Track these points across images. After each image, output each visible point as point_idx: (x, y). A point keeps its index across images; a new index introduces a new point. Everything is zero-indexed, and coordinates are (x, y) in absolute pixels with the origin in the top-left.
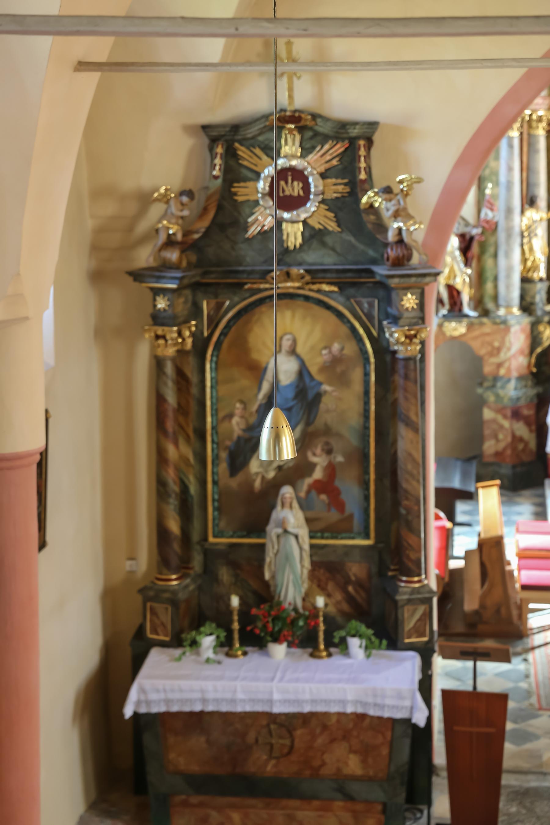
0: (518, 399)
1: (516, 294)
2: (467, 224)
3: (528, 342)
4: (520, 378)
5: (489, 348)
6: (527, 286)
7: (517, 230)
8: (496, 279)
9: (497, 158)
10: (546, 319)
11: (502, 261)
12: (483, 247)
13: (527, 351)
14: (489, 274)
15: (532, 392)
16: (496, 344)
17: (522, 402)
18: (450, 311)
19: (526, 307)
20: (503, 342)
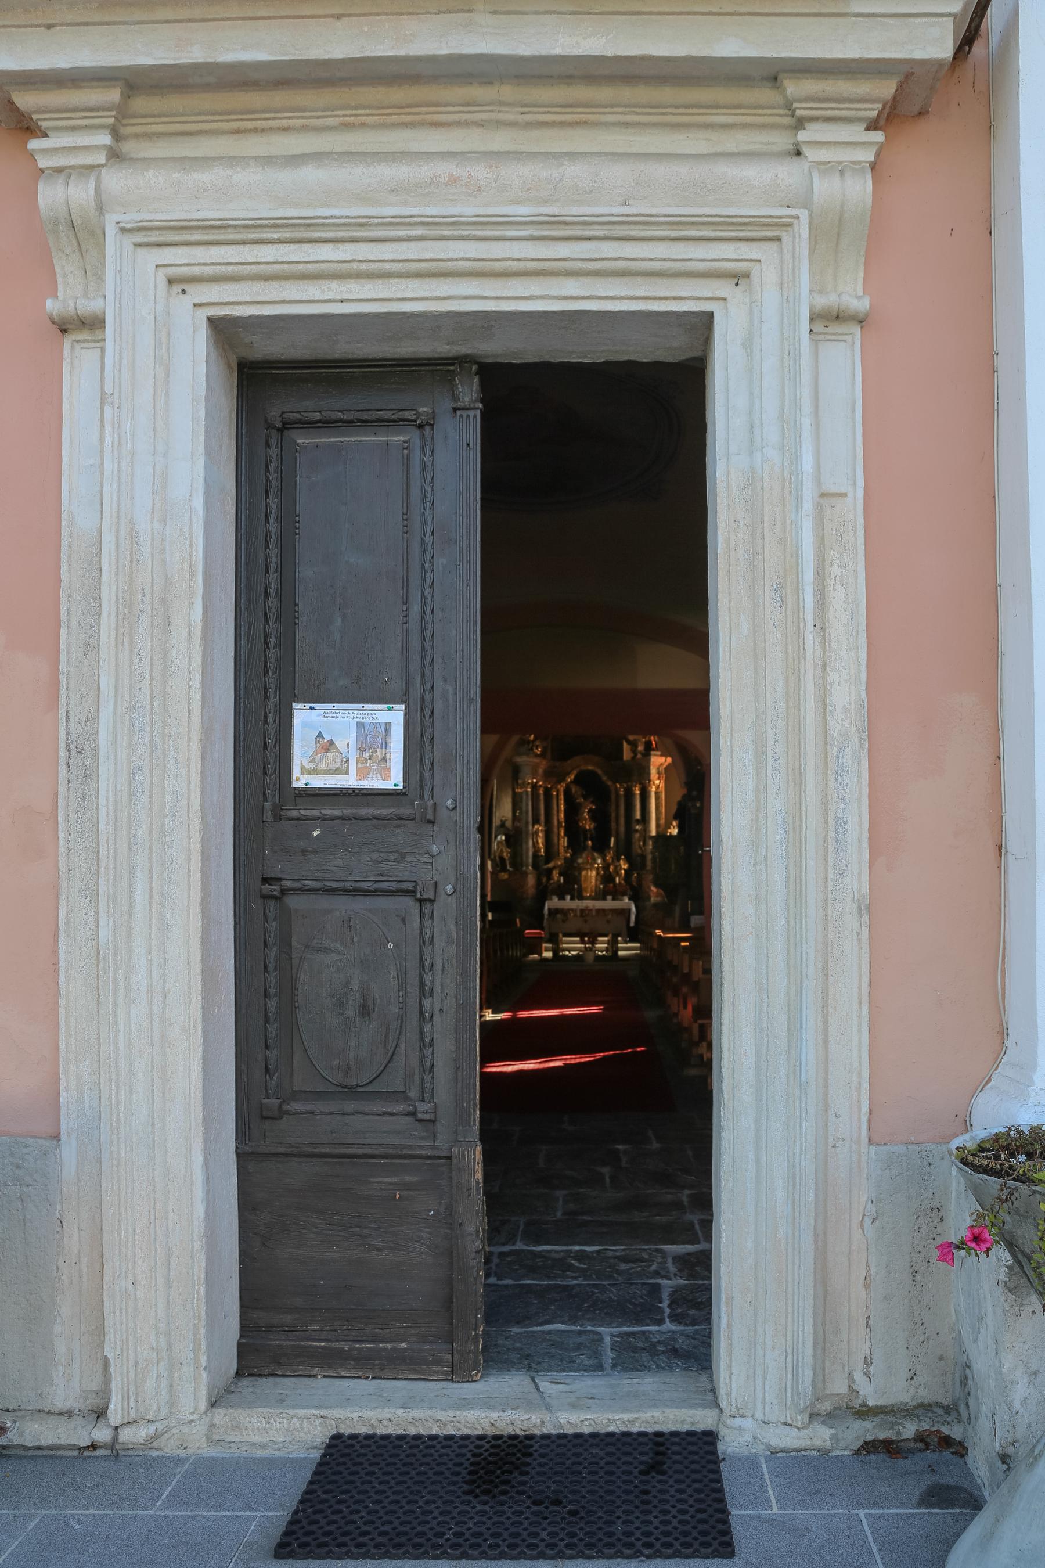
1: (530, 860)
11: (524, 846)
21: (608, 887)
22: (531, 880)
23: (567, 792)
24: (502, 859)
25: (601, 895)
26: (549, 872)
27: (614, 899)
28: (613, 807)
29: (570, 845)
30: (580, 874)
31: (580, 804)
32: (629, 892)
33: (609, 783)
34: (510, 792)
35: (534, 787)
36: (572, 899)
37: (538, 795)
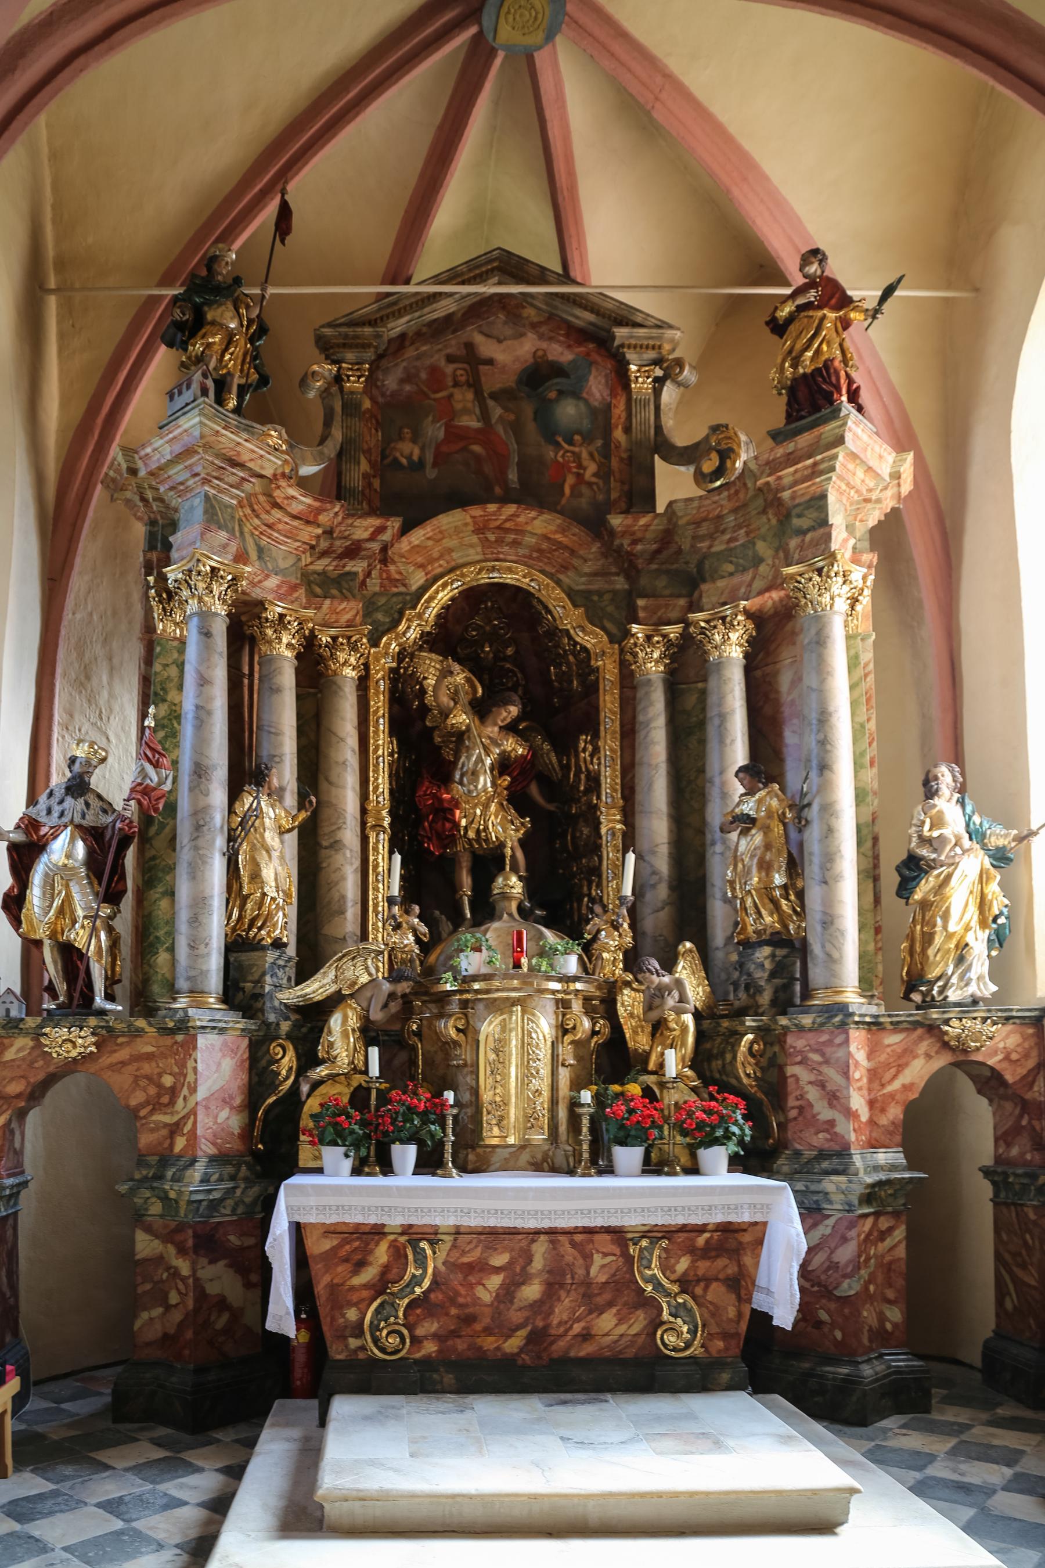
1: (214, 963)
2: (107, 808)
4: (218, 1159)
6: (245, 957)
10: (285, 1026)
11: (184, 890)
16: (168, 1081)
18: (60, 1007)
21: (610, 1107)
22: (215, 1066)
24: (71, 957)
25: (586, 1144)
27: (652, 1166)
29: (414, 890)
32: (741, 1127)
34: (135, 650)
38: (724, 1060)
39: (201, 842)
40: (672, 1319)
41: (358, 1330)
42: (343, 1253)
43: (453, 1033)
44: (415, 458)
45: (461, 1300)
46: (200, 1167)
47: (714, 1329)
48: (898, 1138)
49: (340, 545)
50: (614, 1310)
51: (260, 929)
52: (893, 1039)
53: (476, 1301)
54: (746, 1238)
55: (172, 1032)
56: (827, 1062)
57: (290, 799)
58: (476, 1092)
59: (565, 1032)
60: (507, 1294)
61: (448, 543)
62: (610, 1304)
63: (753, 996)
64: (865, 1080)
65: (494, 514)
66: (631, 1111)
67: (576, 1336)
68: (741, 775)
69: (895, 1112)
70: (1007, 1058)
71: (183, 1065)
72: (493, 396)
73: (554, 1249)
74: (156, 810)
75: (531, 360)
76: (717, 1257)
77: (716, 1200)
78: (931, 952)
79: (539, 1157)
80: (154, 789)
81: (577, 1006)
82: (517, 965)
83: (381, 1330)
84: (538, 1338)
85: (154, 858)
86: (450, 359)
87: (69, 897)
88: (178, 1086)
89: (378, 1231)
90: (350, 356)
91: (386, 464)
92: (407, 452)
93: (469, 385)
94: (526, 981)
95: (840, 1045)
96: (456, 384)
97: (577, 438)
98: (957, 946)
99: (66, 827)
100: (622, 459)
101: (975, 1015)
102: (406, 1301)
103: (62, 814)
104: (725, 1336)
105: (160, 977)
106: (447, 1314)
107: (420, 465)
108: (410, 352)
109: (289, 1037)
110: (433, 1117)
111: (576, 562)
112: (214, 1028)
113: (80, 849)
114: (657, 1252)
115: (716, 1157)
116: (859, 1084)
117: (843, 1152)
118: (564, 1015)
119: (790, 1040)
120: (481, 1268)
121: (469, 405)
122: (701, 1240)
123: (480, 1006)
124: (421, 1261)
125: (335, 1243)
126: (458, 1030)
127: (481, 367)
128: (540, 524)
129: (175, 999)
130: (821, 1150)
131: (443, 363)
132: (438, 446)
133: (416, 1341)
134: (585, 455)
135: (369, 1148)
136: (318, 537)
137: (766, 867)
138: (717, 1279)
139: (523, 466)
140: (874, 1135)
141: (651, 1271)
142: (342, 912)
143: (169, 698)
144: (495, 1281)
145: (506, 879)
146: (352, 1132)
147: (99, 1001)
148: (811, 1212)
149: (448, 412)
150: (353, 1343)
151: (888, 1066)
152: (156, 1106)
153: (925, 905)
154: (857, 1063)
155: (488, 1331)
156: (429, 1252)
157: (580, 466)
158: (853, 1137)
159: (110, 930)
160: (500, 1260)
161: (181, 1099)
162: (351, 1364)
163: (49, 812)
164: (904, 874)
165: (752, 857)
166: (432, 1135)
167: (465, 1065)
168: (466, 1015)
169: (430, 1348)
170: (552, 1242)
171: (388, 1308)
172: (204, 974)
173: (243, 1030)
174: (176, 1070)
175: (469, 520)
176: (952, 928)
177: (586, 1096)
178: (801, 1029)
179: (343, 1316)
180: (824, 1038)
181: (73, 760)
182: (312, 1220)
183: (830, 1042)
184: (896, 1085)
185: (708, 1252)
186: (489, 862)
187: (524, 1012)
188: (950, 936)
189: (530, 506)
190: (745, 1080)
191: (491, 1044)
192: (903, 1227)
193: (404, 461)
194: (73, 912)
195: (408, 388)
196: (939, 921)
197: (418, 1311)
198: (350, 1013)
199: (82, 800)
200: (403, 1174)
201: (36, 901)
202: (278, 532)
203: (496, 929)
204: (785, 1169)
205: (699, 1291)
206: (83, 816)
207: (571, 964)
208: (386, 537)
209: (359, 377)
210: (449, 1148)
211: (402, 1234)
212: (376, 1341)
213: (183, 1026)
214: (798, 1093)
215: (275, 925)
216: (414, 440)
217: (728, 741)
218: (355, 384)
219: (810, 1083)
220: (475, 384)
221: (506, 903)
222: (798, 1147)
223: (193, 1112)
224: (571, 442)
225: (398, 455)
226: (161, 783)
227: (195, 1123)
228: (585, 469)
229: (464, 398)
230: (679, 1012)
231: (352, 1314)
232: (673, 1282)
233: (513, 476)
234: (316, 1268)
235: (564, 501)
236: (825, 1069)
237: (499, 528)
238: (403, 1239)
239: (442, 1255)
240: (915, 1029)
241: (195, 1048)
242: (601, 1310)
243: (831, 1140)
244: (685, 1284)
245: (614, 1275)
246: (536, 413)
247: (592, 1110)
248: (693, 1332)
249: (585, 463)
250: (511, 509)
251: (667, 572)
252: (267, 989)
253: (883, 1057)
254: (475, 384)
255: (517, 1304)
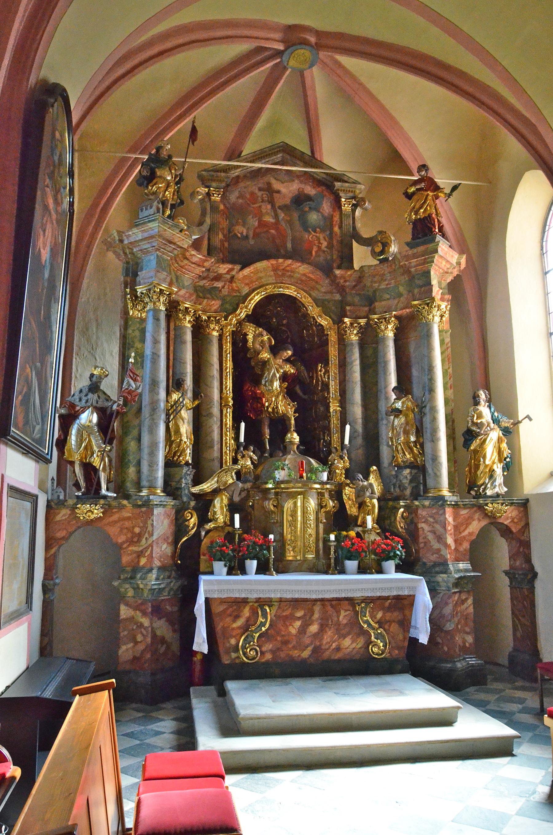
0: (161, 590)
1: (160, 474)
2: (108, 399)
3: (173, 527)
5: (129, 535)
7: (162, 405)
8: (139, 463)
9: (143, 340)
10: (193, 503)
12: (126, 428)
13: (170, 541)
14: (132, 458)
15: (175, 584)
16: (137, 530)
17: (165, 596)
19: (171, 489)
20: (144, 527)
22: (161, 522)
23: (239, 339)
24: (90, 470)
26: (204, 503)
27: (362, 570)
28: (333, 370)
30: (279, 507)
31: (264, 364)
33: (324, 322)
35: (173, 308)
36: (262, 569)
37: (179, 330)
38: (391, 520)
39: (155, 417)
40: (376, 640)
41: (236, 649)
42: (229, 612)
43: (272, 508)
44: (245, 234)
45: (283, 633)
46: (155, 571)
47: (394, 645)
48: (468, 557)
49: (212, 275)
50: (350, 637)
51: (179, 457)
52: (464, 512)
53: (289, 633)
54: (406, 602)
55: (140, 506)
56: (436, 522)
57: (190, 394)
58: (282, 534)
59: (322, 507)
60: (303, 630)
61: (260, 275)
62: (348, 634)
63: (402, 491)
64: (453, 530)
65: (281, 263)
66: (353, 544)
67: (334, 649)
68: (395, 391)
69: (466, 545)
70: (512, 521)
71: (145, 523)
72: (280, 208)
73: (324, 608)
74: (134, 401)
75: (297, 192)
76: (394, 611)
77: (393, 585)
78: (479, 473)
79: (311, 565)
80: (134, 391)
81: (327, 495)
82: (301, 477)
83: (247, 649)
84: (316, 650)
85: (128, 422)
86: (260, 189)
87: (90, 441)
88: (143, 533)
89: (245, 601)
90: (214, 184)
91: (230, 236)
92: (240, 231)
93: (269, 203)
94: (305, 485)
95: (441, 515)
96: (263, 201)
97: (318, 230)
98: (489, 470)
99: (89, 407)
100: (338, 241)
101: (498, 502)
102: (258, 634)
103: (87, 401)
104: (398, 648)
105: (130, 479)
106: (276, 640)
107: (247, 237)
108: (242, 185)
109: (194, 509)
110: (265, 547)
111: (318, 286)
112: (161, 505)
113: (95, 418)
114: (368, 610)
115: (390, 565)
116: (450, 532)
117: (445, 564)
118: (321, 499)
119: (420, 512)
120: (292, 618)
121: (269, 211)
122: (387, 603)
123: (284, 495)
124: (265, 615)
125: (225, 607)
126: (274, 506)
127: (274, 194)
128: (302, 269)
129: (140, 491)
130: (435, 562)
131: (257, 191)
132: (254, 231)
133: (263, 653)
134: (321, 237)
135: (235, 562)
136: (203, 272)
137: (407, 433)
138: (394, 621)
139: (293, 240)
140: (457, 555)
141: (367, 619)
142: (212, 447)
143: (135, 346)
144: (298, 624)
145: (292, 435)
146: (228, 554)
147: (104, 491)
148: (433, 591)
149: (259, 215)
150: (234, 655)
151: (462, 524)
152: (131, 542)
153: (475, 452)
154: (449, 523)
155: (294, 648)
156: (268, 610)
157: (319, 243)
158: (449, 556)
159: (108, 456)
160: (299, 614)
161: (144, 539)
162: (232, 666)
163: (80, 400)
164: (466, 438)
165: (400, 428)
166: (264, 555)
167: (277, 522)
168: (277, 499)
169: (268, 656)
170: (323, 605)
171: (250, 639)
172: (156, 478)
173: (173, 505)
174: (142, 525)
175: (270, 265)
176: (487, 462)
177: (332, 537)
178: (424, 506)
179: (229, 642)
180: (434, 511)
181: (92, 375)
182: (216, 596)
183: (437, 513)
184: (466, 533)
185: (390, 609)
186: (280, 425)
187: (304, 498)
188: (486, 466)
189: (297, 261)
190: (400, 530)
191: (289, 513)
192: (472, 598)
193: (239, 235)
194: (92, 448)
195: (240, 201)
196: (482, 460)
197: (263, 639)
198: (224, 497)
199: (96, 395)
200: (251, 574)
201: (73, 443)
202: (185, 269)
203: (289, 459)
204: (420, 571)
205: (386, 627)
206: (97, 403)
207: (325, 476)
208: (234, 273)
209: (218, 195)
210: (271, 561)
211: (256, 602)
212: (245, 654)
213: (147, 504)
214: (424, 536)
215: (186, 455)
216: (244, 226)
217: (388, 374)
218: (216, 198)
219: (429, 531)
220: (271, 202)
221: (292, 446)
222: (424, 560)
223: (151, 545)
224: (315, 232)
225: (236, 232)
226: (137, 388)
227: (152, 550)
228: (322, 244)
229: (267, 208)
230: (371, 498)
231: (233, 641)
232: (376, 623)
233: (289, 245)
234: (216, 619)
235: (312, 258)
236: (435, 525)
237: (283, 269)
238: (256, 605)
239: (273, 612)
240: (473, 508)
241: (153, 514)
242: (344, 637)
243: (439, 558)
244: (381, 624)
245: (350, 620)
246: (299, 217)
247: (335, 544)
248: (385, 646)
249: (321, 242)
250: (289, 262)
251: (359, 295)
252: (183, 485)
253: (460, 520)
254: (271, 202)
255: (308, 634)
